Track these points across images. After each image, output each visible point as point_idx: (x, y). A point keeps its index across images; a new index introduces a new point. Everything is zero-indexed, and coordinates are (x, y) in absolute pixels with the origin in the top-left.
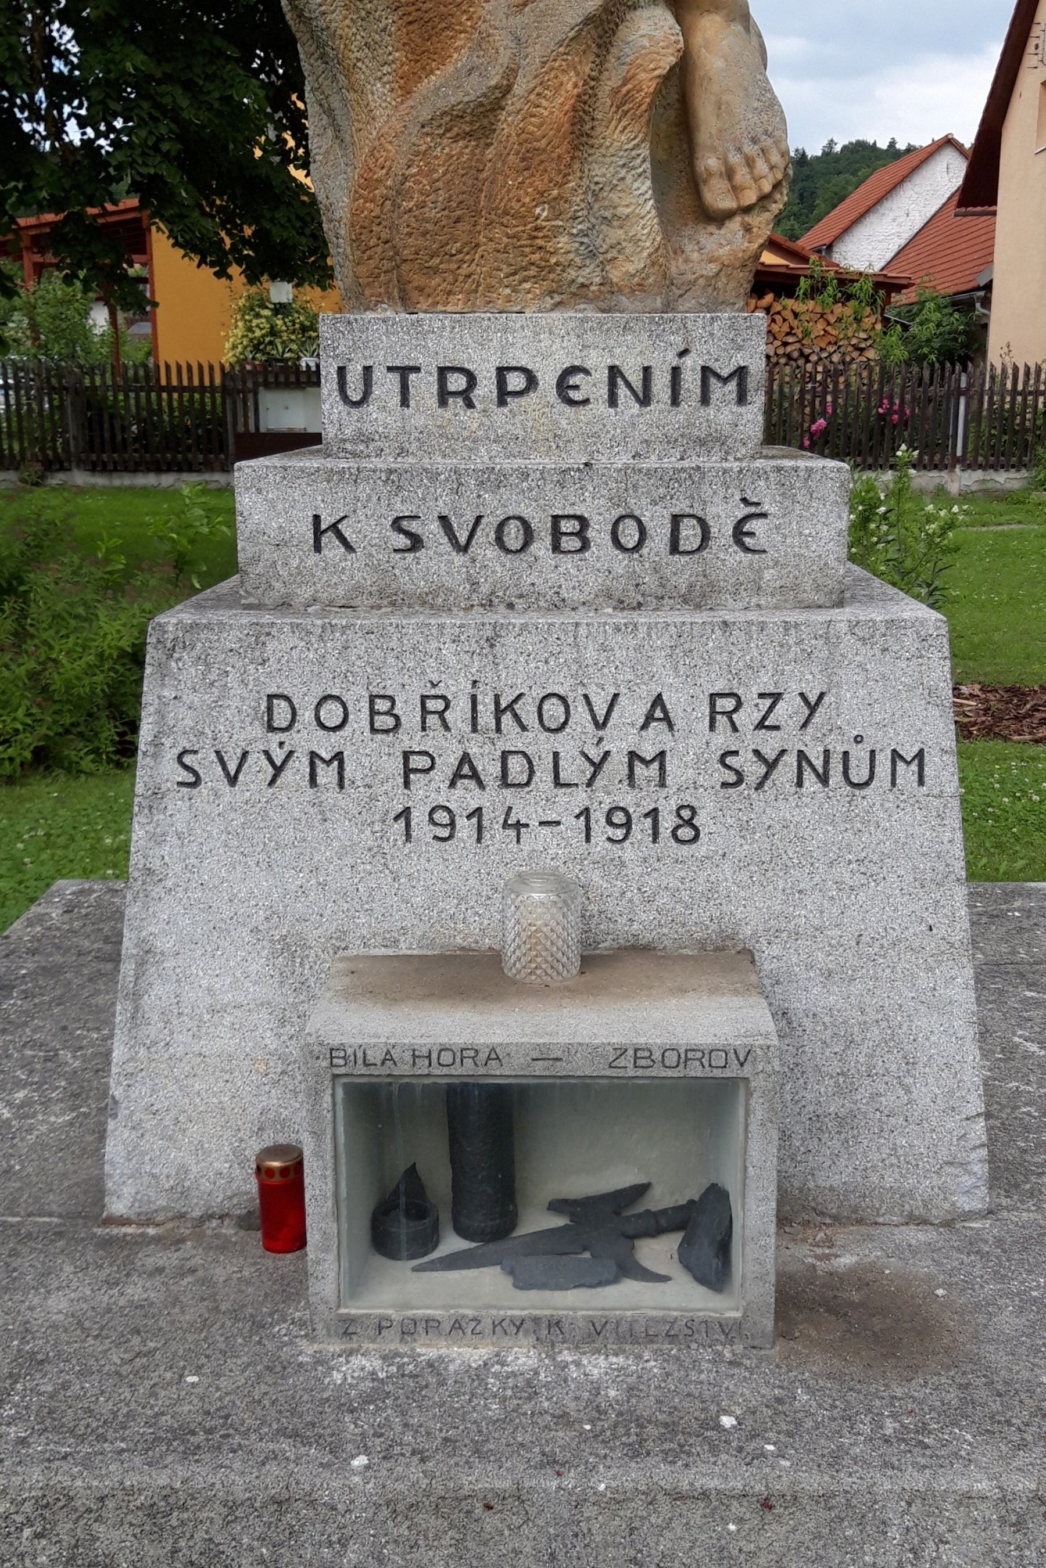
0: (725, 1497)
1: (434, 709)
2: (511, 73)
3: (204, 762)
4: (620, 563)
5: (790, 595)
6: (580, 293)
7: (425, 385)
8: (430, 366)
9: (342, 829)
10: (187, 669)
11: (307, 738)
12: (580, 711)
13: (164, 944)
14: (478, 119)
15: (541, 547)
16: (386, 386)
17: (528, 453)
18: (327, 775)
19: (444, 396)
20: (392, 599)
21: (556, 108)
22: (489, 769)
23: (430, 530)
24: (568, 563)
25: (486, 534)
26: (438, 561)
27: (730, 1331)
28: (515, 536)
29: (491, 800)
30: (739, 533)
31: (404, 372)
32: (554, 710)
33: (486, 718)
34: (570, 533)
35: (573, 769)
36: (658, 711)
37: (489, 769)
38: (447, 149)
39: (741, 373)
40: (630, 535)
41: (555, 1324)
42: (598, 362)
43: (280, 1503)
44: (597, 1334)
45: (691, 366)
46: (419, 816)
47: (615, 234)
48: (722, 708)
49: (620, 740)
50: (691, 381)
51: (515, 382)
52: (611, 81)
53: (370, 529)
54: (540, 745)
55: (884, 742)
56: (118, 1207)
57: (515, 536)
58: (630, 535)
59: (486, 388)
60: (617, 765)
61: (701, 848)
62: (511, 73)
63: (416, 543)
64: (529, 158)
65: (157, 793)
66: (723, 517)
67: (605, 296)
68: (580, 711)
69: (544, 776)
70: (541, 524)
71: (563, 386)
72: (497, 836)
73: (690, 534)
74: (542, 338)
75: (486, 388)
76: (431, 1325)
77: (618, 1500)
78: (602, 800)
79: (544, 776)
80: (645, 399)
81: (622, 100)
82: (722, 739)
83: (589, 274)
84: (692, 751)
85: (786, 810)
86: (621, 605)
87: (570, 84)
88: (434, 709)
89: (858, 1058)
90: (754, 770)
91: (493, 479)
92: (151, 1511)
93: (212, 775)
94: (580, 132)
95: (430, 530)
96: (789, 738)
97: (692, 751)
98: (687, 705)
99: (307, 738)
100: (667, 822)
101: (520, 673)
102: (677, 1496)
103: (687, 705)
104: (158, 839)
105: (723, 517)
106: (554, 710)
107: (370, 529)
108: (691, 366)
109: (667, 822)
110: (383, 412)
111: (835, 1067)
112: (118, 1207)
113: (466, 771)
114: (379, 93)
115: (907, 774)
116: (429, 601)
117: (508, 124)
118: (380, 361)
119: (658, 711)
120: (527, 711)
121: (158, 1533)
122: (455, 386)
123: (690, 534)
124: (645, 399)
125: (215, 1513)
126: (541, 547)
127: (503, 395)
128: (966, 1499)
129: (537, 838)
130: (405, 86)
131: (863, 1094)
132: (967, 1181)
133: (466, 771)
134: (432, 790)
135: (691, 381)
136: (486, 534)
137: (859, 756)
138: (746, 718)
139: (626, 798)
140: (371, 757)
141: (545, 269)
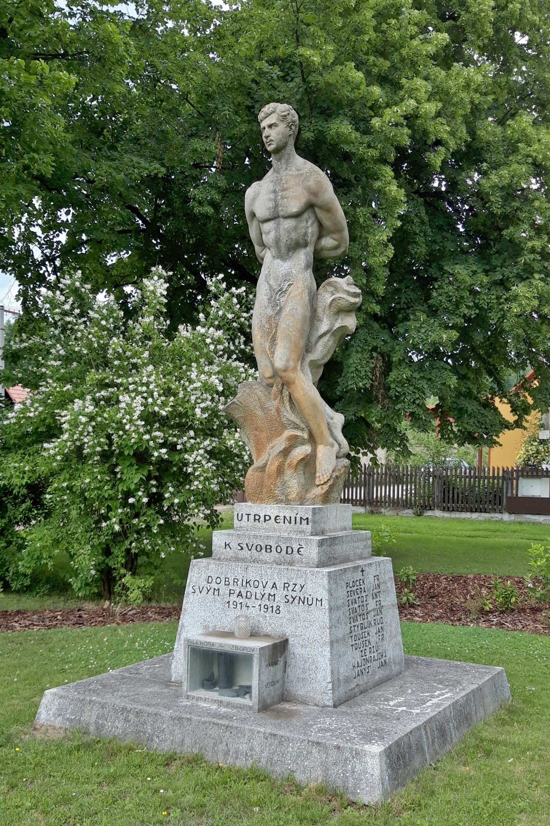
0: (222, 725)
1: (235, 581)
2: (267, 461)
3: (196, 588)
4: (277, 555)
5: (308, 565)
6: (281, 501)
7: (252, 518)
8: (253, 514)
9: (218, 604)
10: (196, 570)
12: (261, 585)
13: (186, 624)
15: (263, 551)
16: (245, 517)
18: (216, 593)
19: (255, 520)
20: (237, 559)
21: (274, 467)
22: (244, 595)
23: (245, 546)
24: (268, 555)
25: (254, 548)
26: (245, 553)
27: (251, 708)
28: (259, 548)
30: (298, 551)
31: (248, 515)
32: (256, 583)
33: (244, 584)
34: (268, 548)
36: (274, 586)
37: (244, 595)
38: (257, 474)
39: (307, 519)
40: (279, 550)
41: (221, 702)
42: (282, 515)
43: (156, 714)
44: (228, 705)
45: (298, 517)
46: (231, 603)
47: (289, 490)
48: (286, 586)
49: (268, 591)
50: (298, 520)
51: (267, 518)
52: (288, 461)
54: (254, 590)
55: (315, 596)
56: (173, 680)
57: (259, 548)
58: (279, 550)
59: (262, 519)
60: (266, 596)
61: (280, 615)
62: (267, 461)
63: (242, 549)
64: (270, 477)
65: (188, 594)
66: (296, 547)
67: (288, 502)
68: (261, 585)
69: (253, 597)
70: (264, 547)
71: (275, 519)
72: (244, 608)
73: (290, 550)
74: (271, 509)
76: (201, 698)
77: (205, 723)
79: (253, 597)
80: (290, 523)
81: (290, 465)
82: (285, 593)
83: (283, 497)
84: (280, 593)
85: (296, 608)
86: (277, 564)
87: (277, 463)
88: (235, 581)
89: (307, 665)
90: (291, 600)
91: (255, 537)
92: (137, 713)
93: (197, 591)
95: (245, 546)
97: (280, 593)
98: (280, 585)
100: (275, 609)
101: (252, 575)
102: (214, 723)
104: (187, 603)
105: (296, 547)
106: (256, 583)
107: (234, 545)
108: (298, 517)
109: (275, 609)
110: (244, 523)
111: (302, 667)
112: (173, 680)
113: (240, 594)
115: (319, 603)
116: (243, 560)
119: (274, 586)
120: (252, 583)
121: (137, 717)
122: (257, 518)
123: (290, 550)
124: (290, 523)
125: (146, 715)
126: (263, 551)
127: (265, 520)
128: (259, 732)
129: (251, 610)
131: (307, 674)
132: (328, 698)
134: (234, 598)
135: (298, 520)
136: (254, 548)
137: (310, 598)
138: (290, 588)
139: (268, 603)
140: (224, 590)
141: (274, 497)
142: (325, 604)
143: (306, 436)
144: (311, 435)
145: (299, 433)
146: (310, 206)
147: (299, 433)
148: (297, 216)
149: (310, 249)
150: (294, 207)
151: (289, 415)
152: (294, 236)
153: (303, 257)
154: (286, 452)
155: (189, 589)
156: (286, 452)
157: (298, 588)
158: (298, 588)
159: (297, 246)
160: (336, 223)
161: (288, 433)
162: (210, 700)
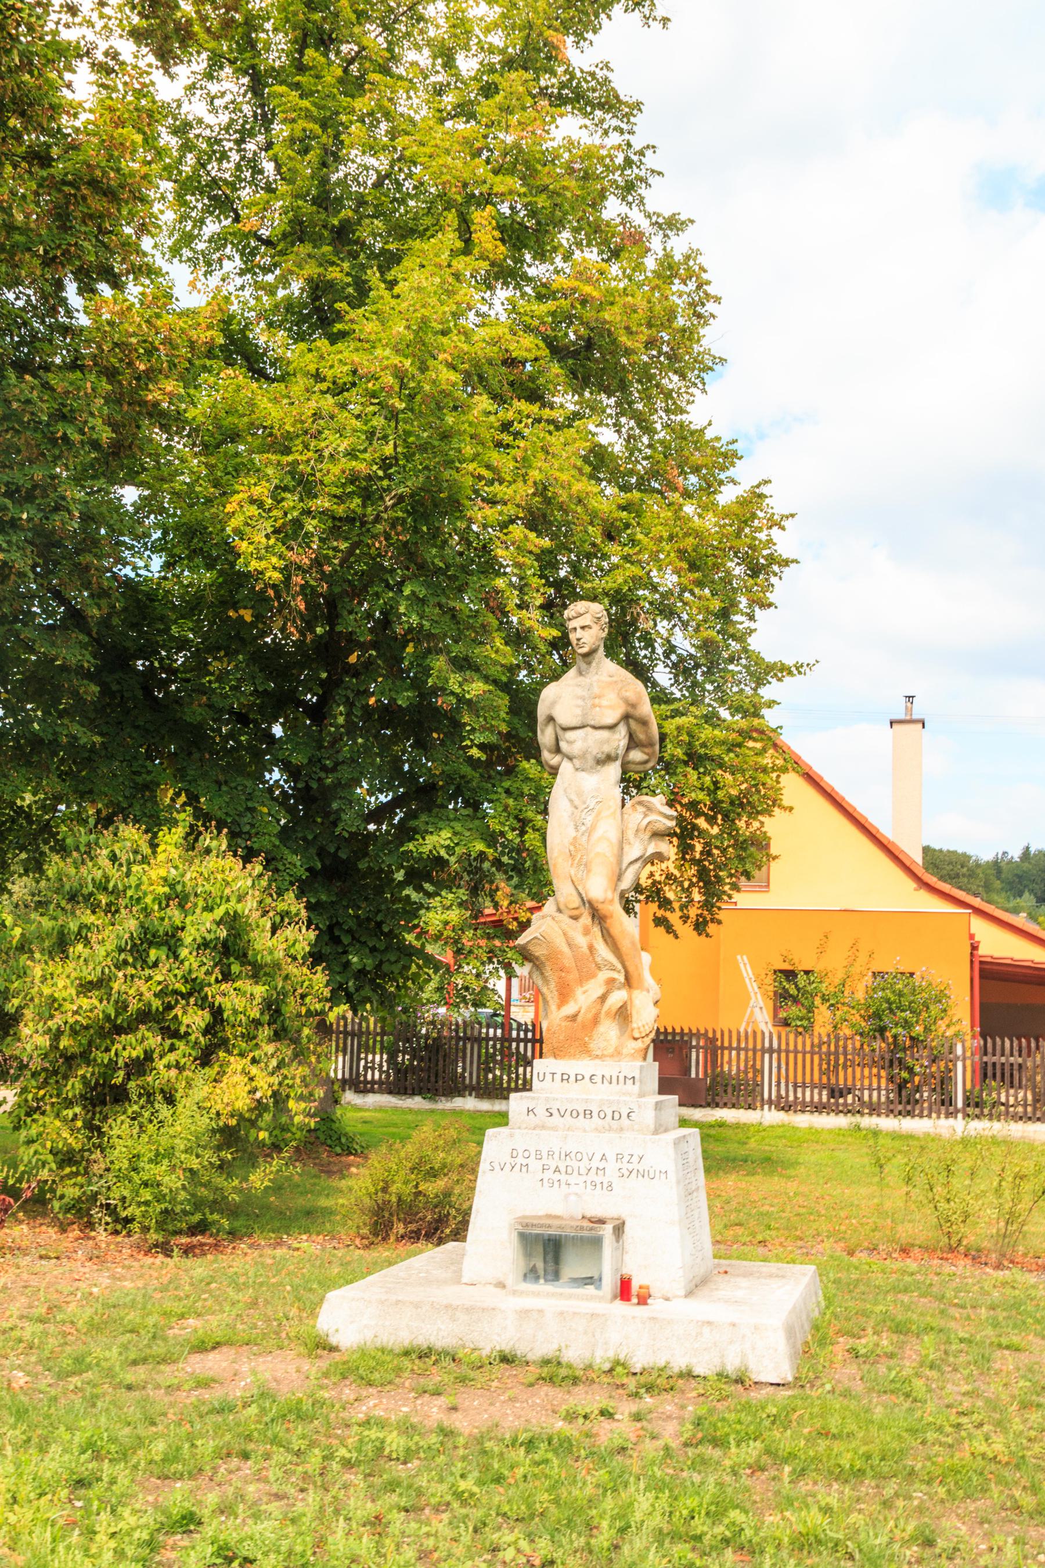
1: (550, 1154)
7: (558, 1077)
11: (520, 1160)
14: (574, 1018)
16: (549, 1077)
17: (574, 1095)
20: (543, 1127)
21: (590, 1016)
28: (575, 1114)
29: (563, 1177)
34: (588, 1114)
35: (583, 1171)
48: (619, 1157)
49: (596, 1163)
53: (541, 1111)
54: (575, 1164)
57: (575, 1114)
59: (572, 1079)
64: (584, 1027)
75: (572, 1079)
78: (589, 1179)
81: (608, 1014)
93: (497, 1168)
94: (595, 1021)
96: (634, 1166)
97: (612, 1166)
98: (611, 1157)
99: (520, 1160)
103: (611, 1157)
107: (541, 1111)
113: (557, 1170)
114: (553, 1007)
116: (555, 1129)
117: (579, 1018)
118: (548, 1071)
122: (565, 1078)
130: (559, 1007)
133: (557, 1170)
140: (535, 1165)
142: (672, 1175)
143: (621, 978)
144: (627, 978)
145: (615, 975)
146: (626, 717)
147: (615, 975)
148: (612, 727)
149: (618, 763)
150: (611, 718)
151: (604, 952)
152: (607, 749)
153: (614, 770)
154: (603, 998)
155: (484, 1167)
156: (603, 998)
157: (635, 1159)
158: (635, 1159)
159: (609, 758)
160: (649, 737)
161: (604, 975)
162: (548, 1298)
